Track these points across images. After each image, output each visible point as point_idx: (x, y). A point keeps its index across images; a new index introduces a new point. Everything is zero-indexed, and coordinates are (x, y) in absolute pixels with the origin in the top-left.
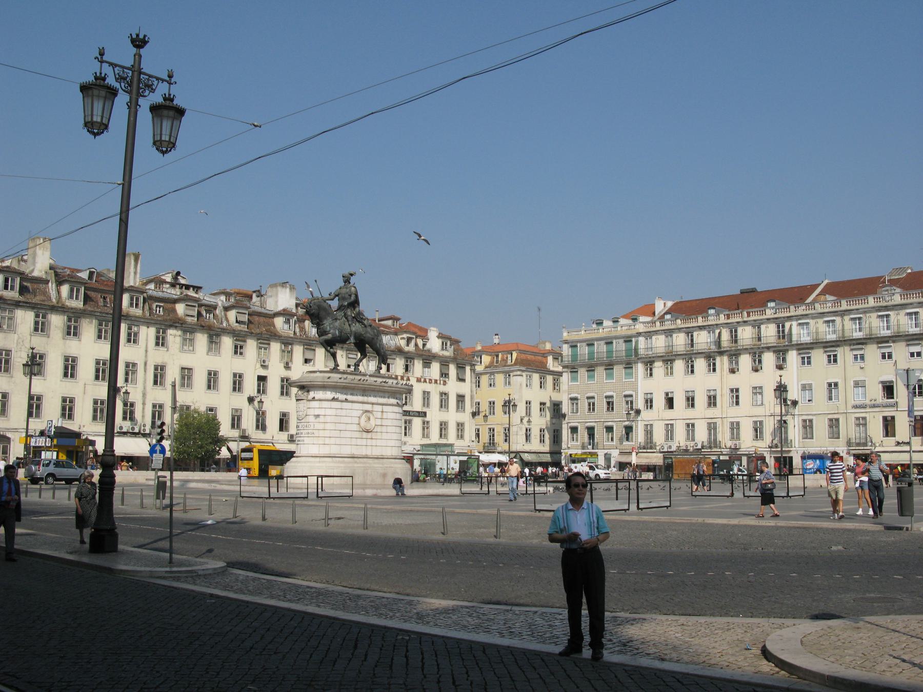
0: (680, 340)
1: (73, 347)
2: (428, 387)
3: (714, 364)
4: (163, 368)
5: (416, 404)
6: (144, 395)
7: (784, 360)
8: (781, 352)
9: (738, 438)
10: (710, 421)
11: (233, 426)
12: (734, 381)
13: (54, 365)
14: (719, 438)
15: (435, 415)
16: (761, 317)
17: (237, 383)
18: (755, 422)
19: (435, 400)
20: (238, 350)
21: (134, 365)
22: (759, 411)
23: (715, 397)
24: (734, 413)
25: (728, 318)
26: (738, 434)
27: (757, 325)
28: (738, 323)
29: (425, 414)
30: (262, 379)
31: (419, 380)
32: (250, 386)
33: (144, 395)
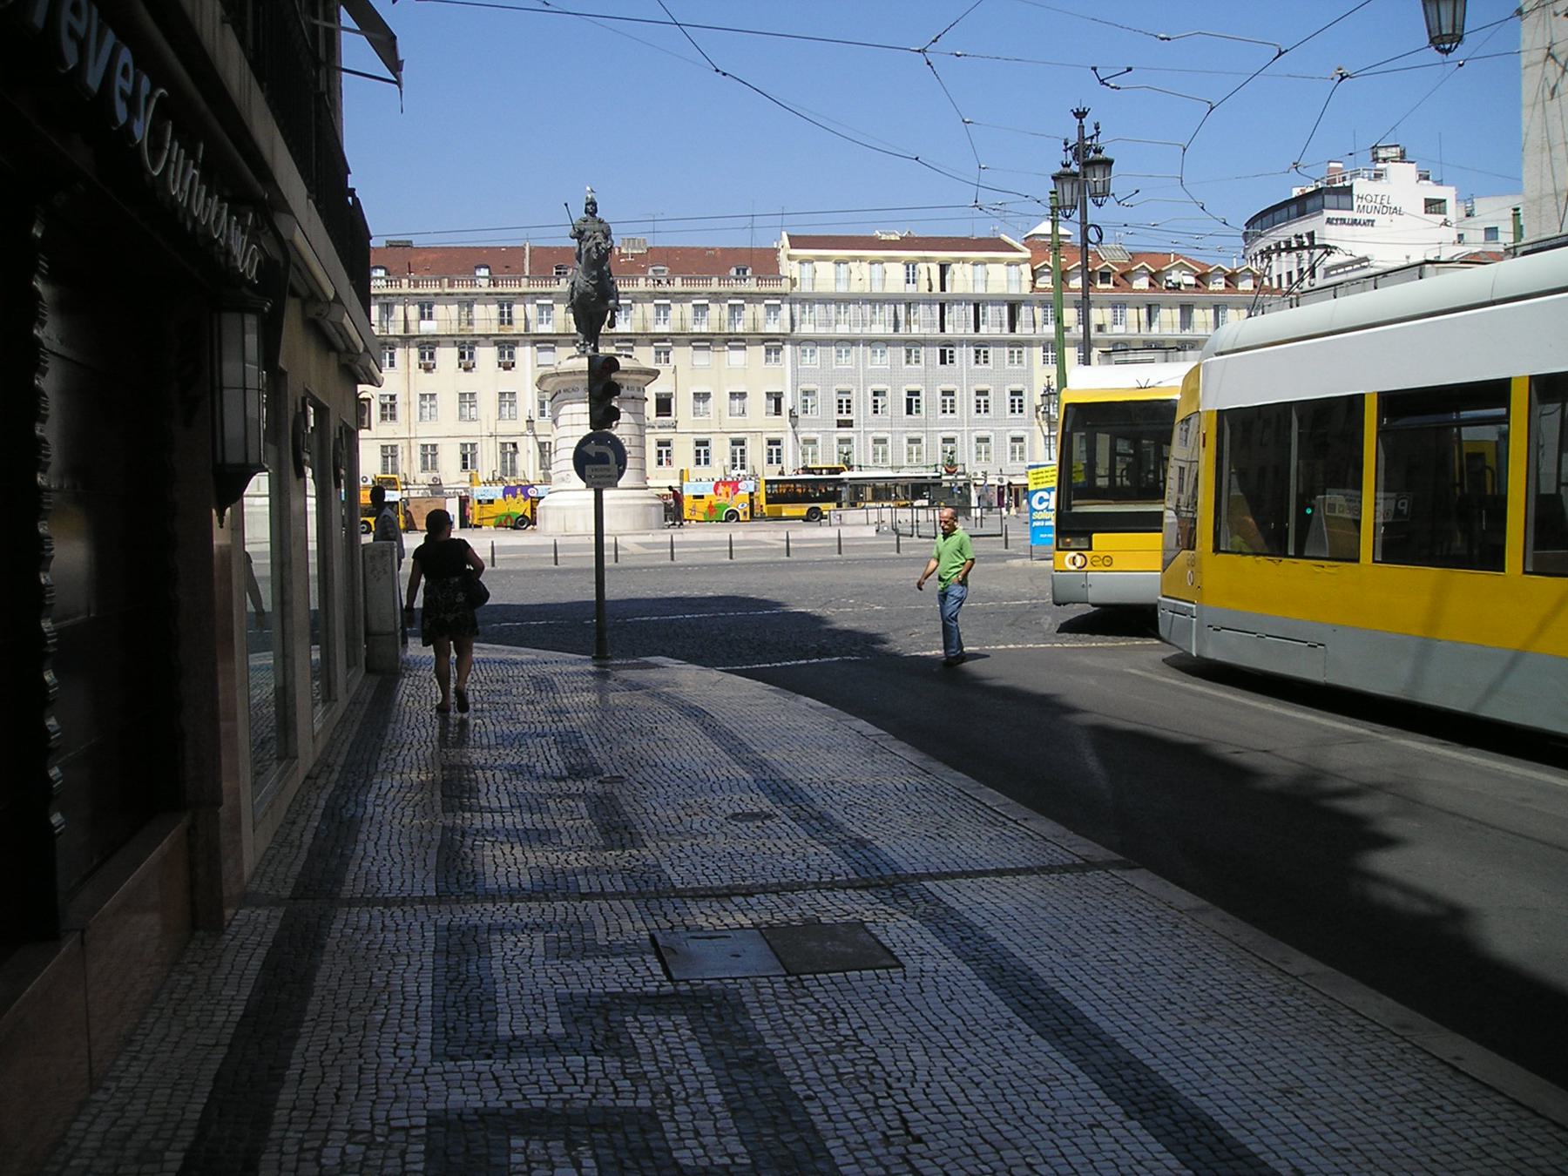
0: (486, 317)
3: (392, 356)
7: (511, 355)
8: (506, 346)
9: (434, 468)
10: (385, 443)
12: (426, 382)
14: (403, 467)
16: (474, 290)
18: (464, 446)
22: (469, 429)
23: (393, 407)
24: (426, 432)
25: (417, 286)
26: (434, 463)
27: (467, 302)
28: (437, 295)
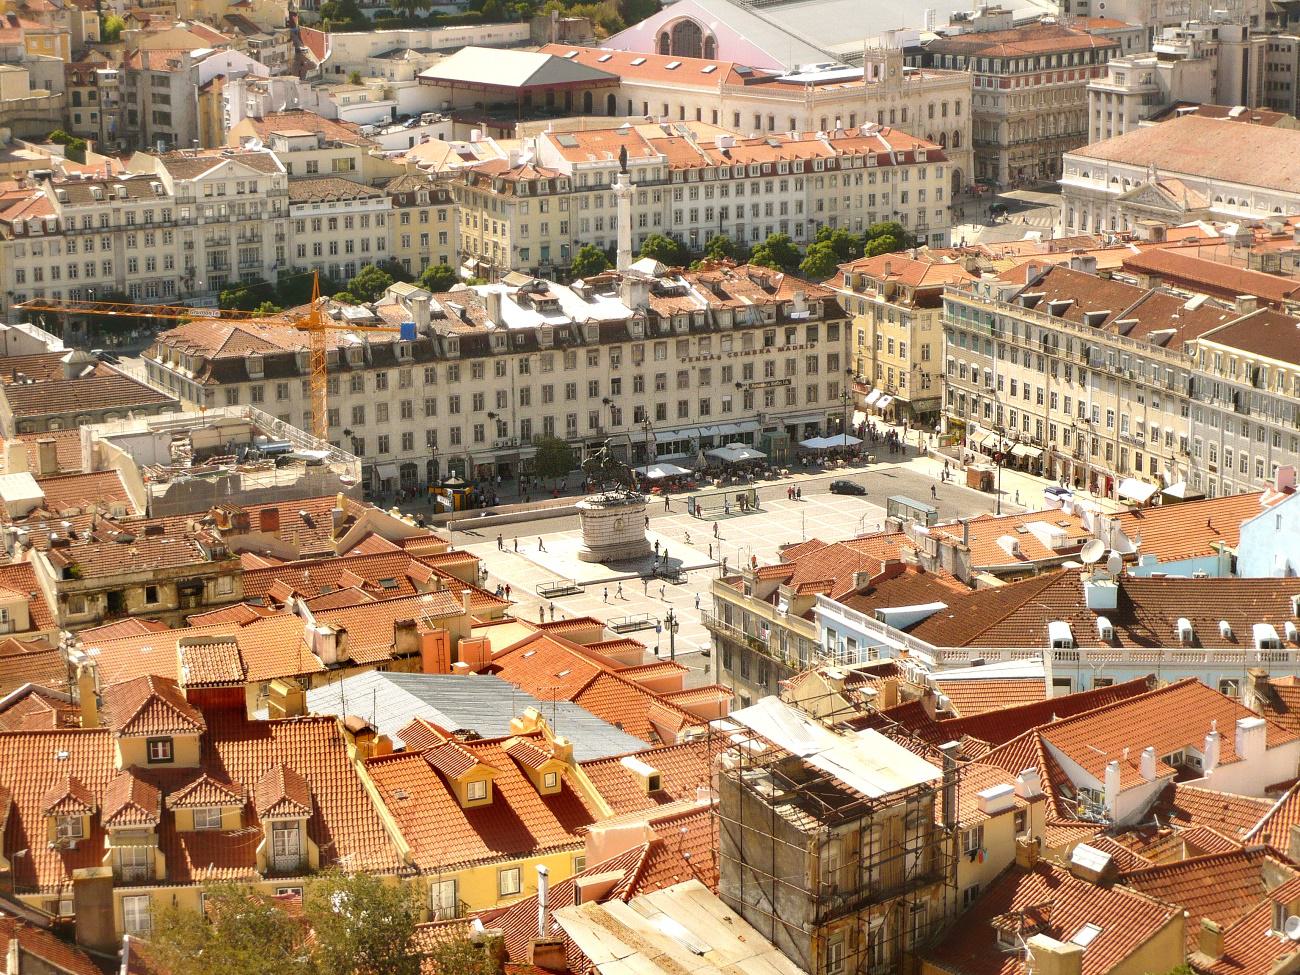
1: (456, 388)
2: (792, 354)
4: (528, 390)
5: (780, 373)
6: (514, 414)
11: (591, 427)
13: (443, 406)
15: (801, 381)
17: (593, 389)
19: (802, 365)
20: (593, 362)
21: (505, 392)
29: (790, 382)
30: (616, 382)
31: (781, 350)
32: (605, 390)
33: (514, 414)
